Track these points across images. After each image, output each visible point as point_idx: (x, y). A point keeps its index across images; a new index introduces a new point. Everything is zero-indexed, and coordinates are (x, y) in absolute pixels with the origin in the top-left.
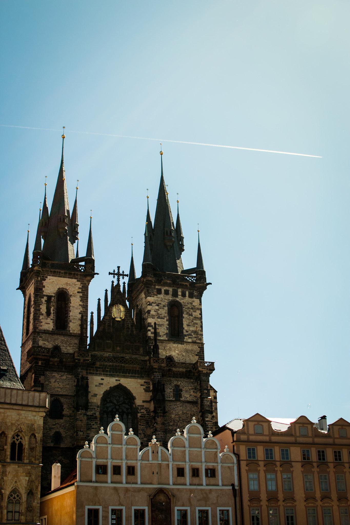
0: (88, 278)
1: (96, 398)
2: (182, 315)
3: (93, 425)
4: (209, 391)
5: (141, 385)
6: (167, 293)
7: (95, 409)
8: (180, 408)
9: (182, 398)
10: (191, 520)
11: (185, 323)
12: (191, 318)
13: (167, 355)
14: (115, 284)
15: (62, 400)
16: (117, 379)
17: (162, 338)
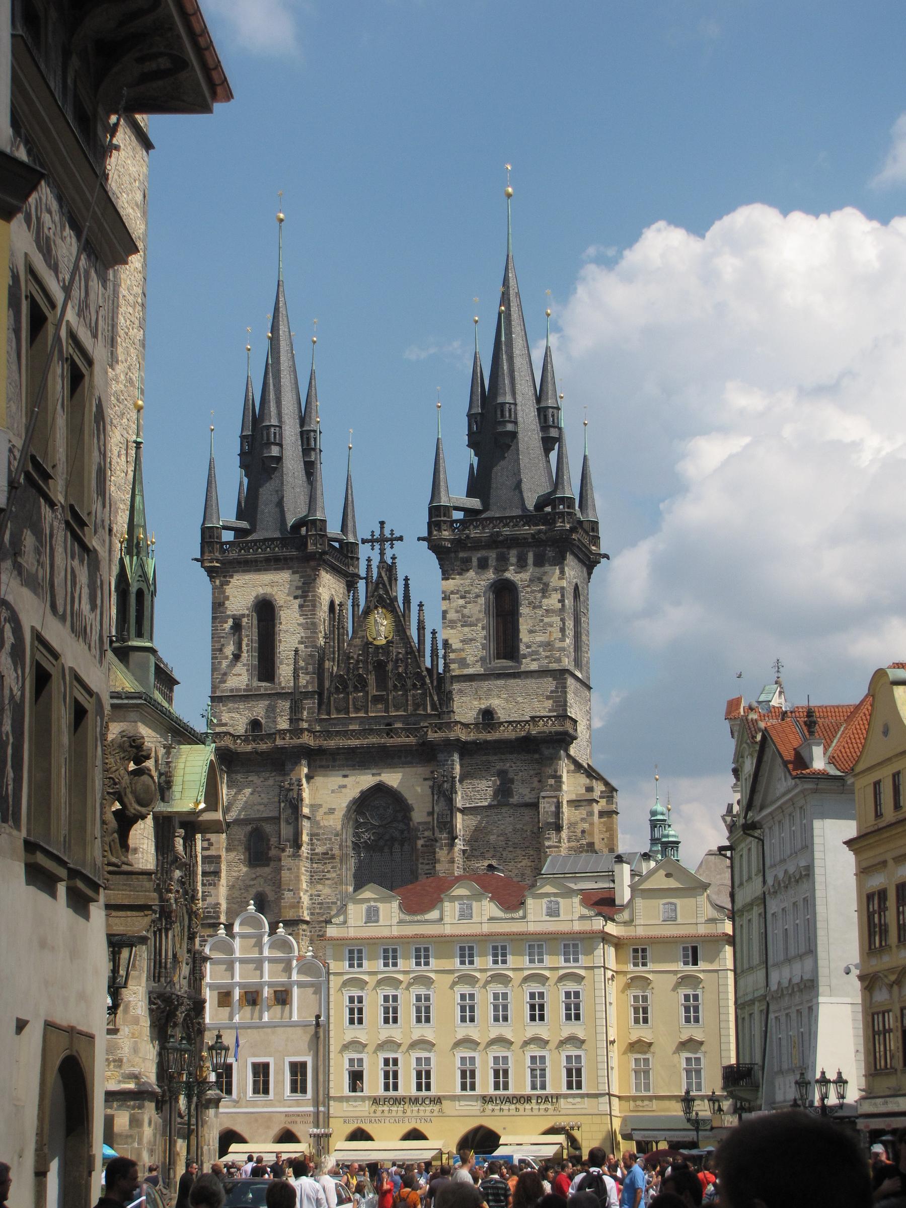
0: (313, 563)
1: (332, 816)
2: (518, 610)
3: (328, 872)
4: (558, 779)
5: (425, 779)
6: (483, 565)
7: (330, 839)
8: (508, 819)
9: (513, 797)
10: (238, 1080)
11: (524, 626)
12: (540, 612)
13: (483, 707)
14: (375, 563)
15: (268, 828)
16: (374, 771)
17: (470, 671)
